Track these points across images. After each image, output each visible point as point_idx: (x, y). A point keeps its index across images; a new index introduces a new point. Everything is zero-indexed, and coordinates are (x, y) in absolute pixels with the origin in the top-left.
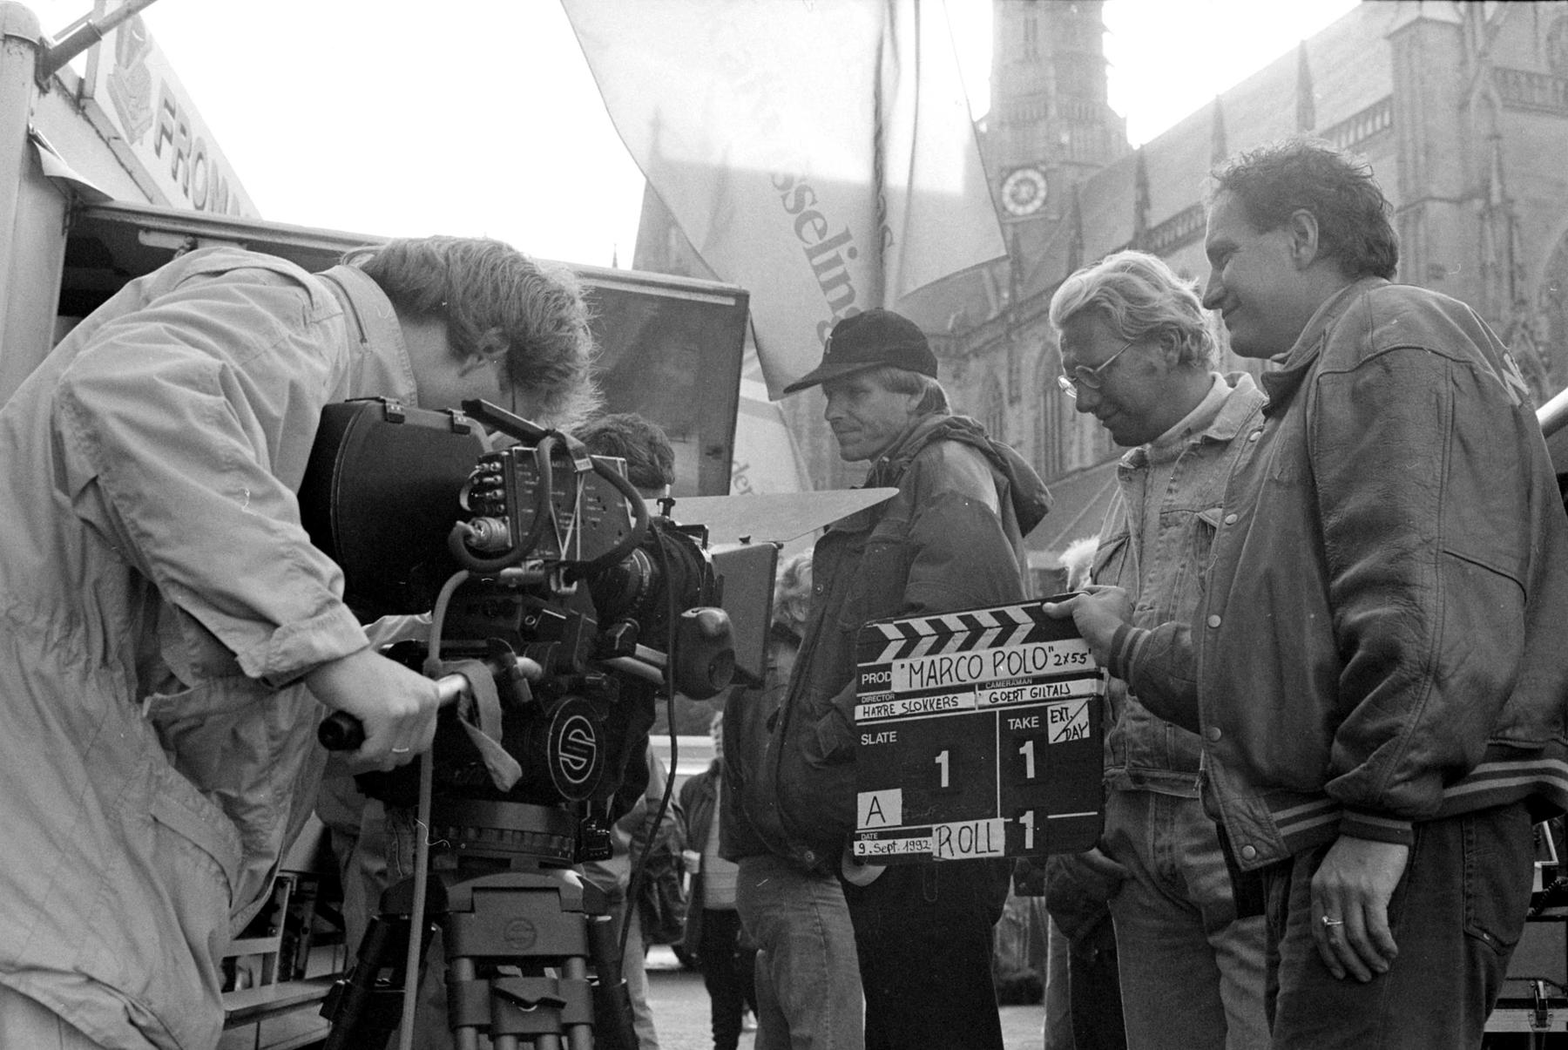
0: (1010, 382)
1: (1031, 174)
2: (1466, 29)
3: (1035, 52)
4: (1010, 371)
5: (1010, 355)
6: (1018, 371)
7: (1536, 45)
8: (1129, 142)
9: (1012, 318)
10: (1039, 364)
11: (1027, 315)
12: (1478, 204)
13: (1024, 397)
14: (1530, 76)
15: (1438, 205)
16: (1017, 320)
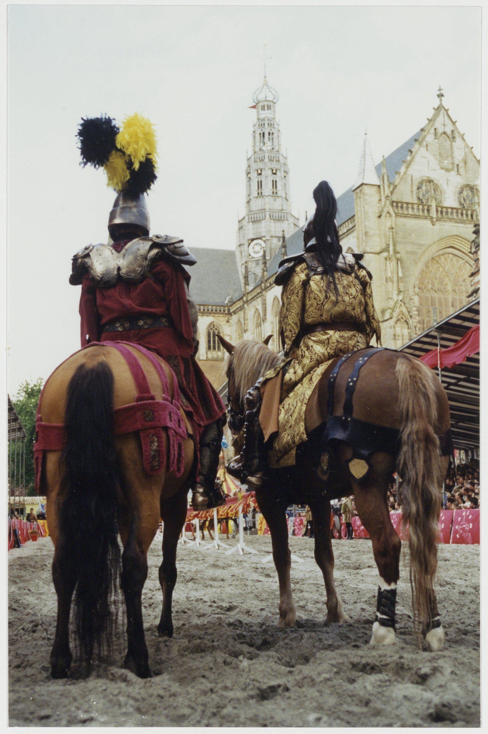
0: (245, 324)
1: (259, 241)
2: (382, 187)
3: (262, 193)
4: (245, 320)
5: (244, 313)
6: (247, 319)
7: (412, 192)
8: (71, 273)
9: (245, 299)
10: (254, 317)
11: (250, 298)
12: (385, 254)
13: (249, 330)
14: (407, 204)
15: (370, 255)
16: (247, 299)
